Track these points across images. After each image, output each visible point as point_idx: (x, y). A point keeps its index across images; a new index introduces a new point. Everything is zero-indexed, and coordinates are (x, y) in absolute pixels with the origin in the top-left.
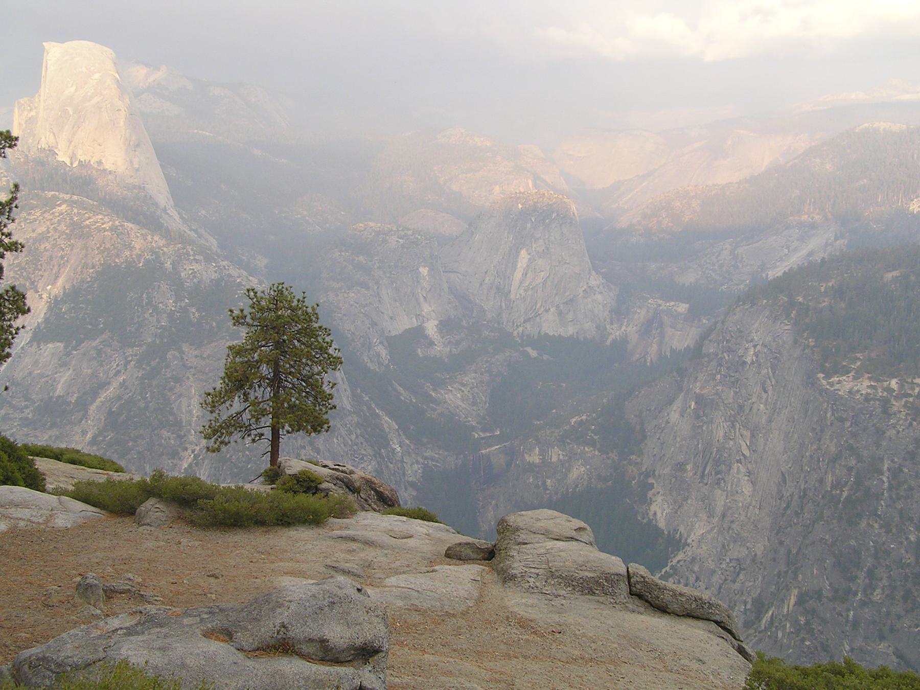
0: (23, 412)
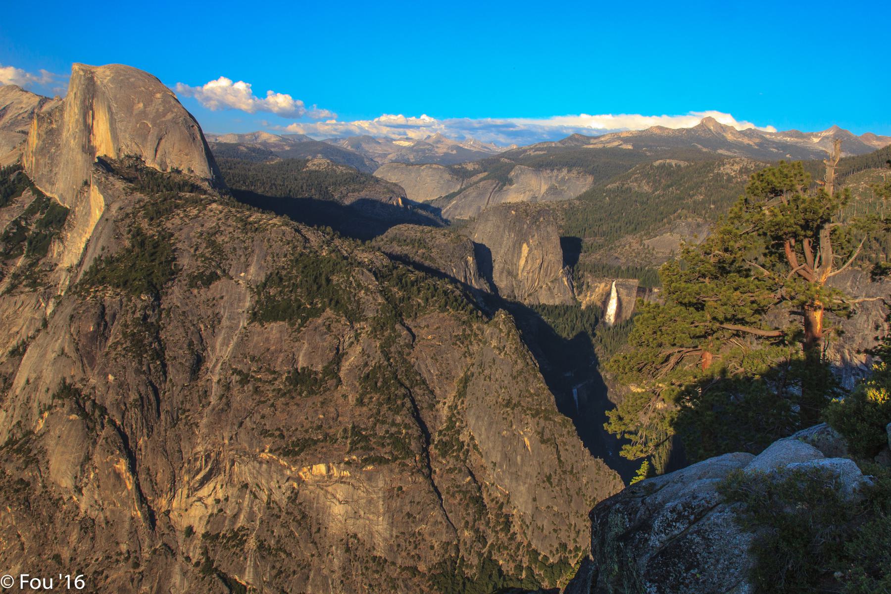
0: (274, 384)
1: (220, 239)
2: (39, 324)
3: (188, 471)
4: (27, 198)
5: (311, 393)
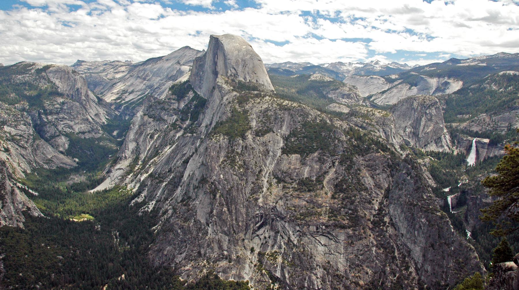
1: (270, 113)
2: (194, 151)
3: (253, 222)
4: (191, 95)
5: (309, 191)
